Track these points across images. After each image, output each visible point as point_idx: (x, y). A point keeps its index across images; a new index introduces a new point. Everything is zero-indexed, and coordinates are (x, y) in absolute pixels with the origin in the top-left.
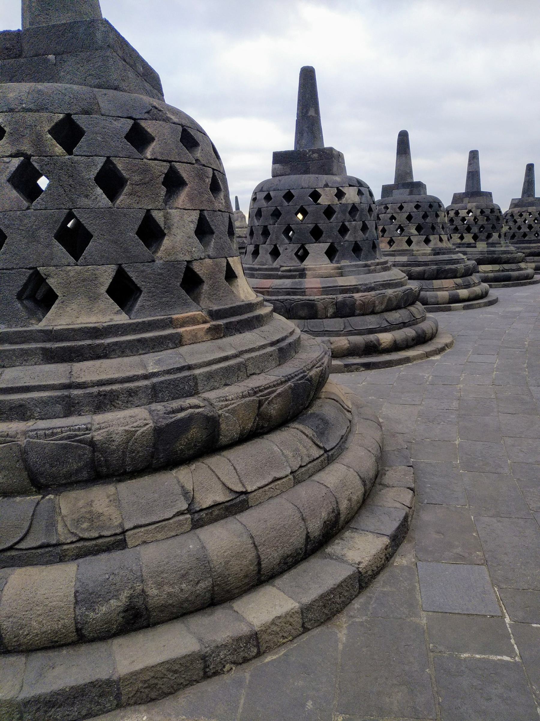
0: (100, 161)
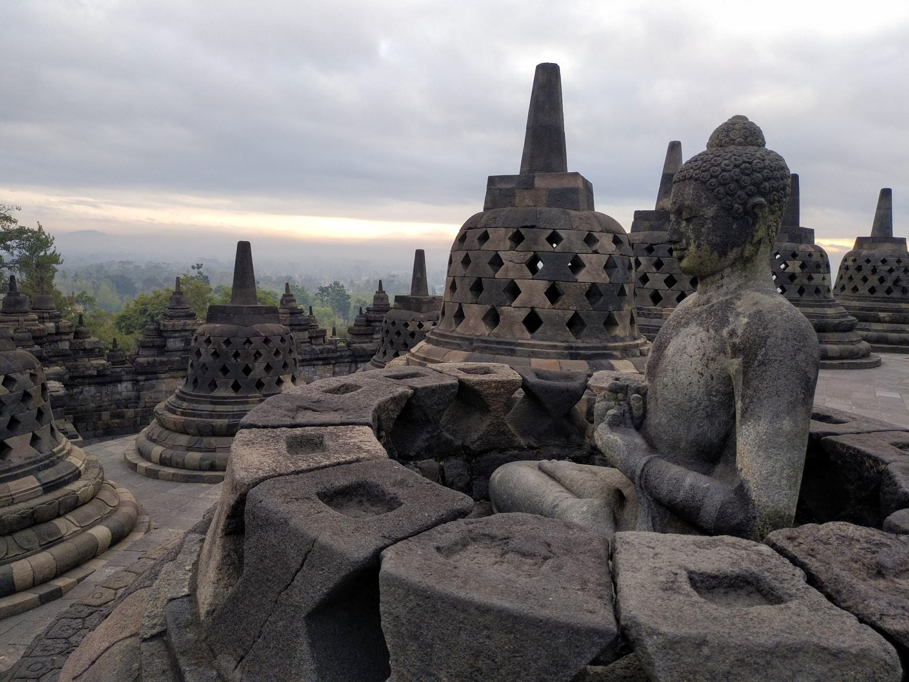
0: (235, 351)
